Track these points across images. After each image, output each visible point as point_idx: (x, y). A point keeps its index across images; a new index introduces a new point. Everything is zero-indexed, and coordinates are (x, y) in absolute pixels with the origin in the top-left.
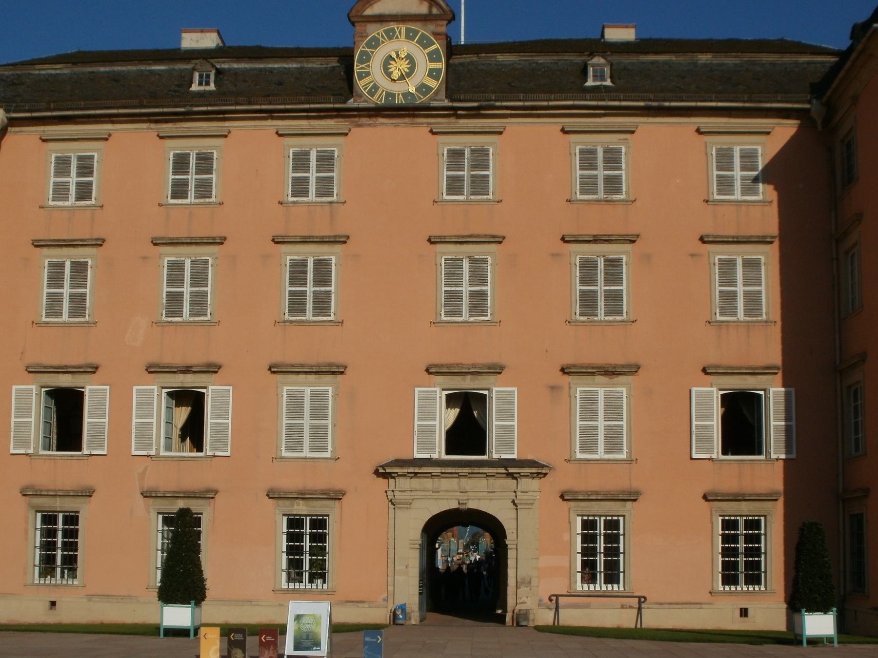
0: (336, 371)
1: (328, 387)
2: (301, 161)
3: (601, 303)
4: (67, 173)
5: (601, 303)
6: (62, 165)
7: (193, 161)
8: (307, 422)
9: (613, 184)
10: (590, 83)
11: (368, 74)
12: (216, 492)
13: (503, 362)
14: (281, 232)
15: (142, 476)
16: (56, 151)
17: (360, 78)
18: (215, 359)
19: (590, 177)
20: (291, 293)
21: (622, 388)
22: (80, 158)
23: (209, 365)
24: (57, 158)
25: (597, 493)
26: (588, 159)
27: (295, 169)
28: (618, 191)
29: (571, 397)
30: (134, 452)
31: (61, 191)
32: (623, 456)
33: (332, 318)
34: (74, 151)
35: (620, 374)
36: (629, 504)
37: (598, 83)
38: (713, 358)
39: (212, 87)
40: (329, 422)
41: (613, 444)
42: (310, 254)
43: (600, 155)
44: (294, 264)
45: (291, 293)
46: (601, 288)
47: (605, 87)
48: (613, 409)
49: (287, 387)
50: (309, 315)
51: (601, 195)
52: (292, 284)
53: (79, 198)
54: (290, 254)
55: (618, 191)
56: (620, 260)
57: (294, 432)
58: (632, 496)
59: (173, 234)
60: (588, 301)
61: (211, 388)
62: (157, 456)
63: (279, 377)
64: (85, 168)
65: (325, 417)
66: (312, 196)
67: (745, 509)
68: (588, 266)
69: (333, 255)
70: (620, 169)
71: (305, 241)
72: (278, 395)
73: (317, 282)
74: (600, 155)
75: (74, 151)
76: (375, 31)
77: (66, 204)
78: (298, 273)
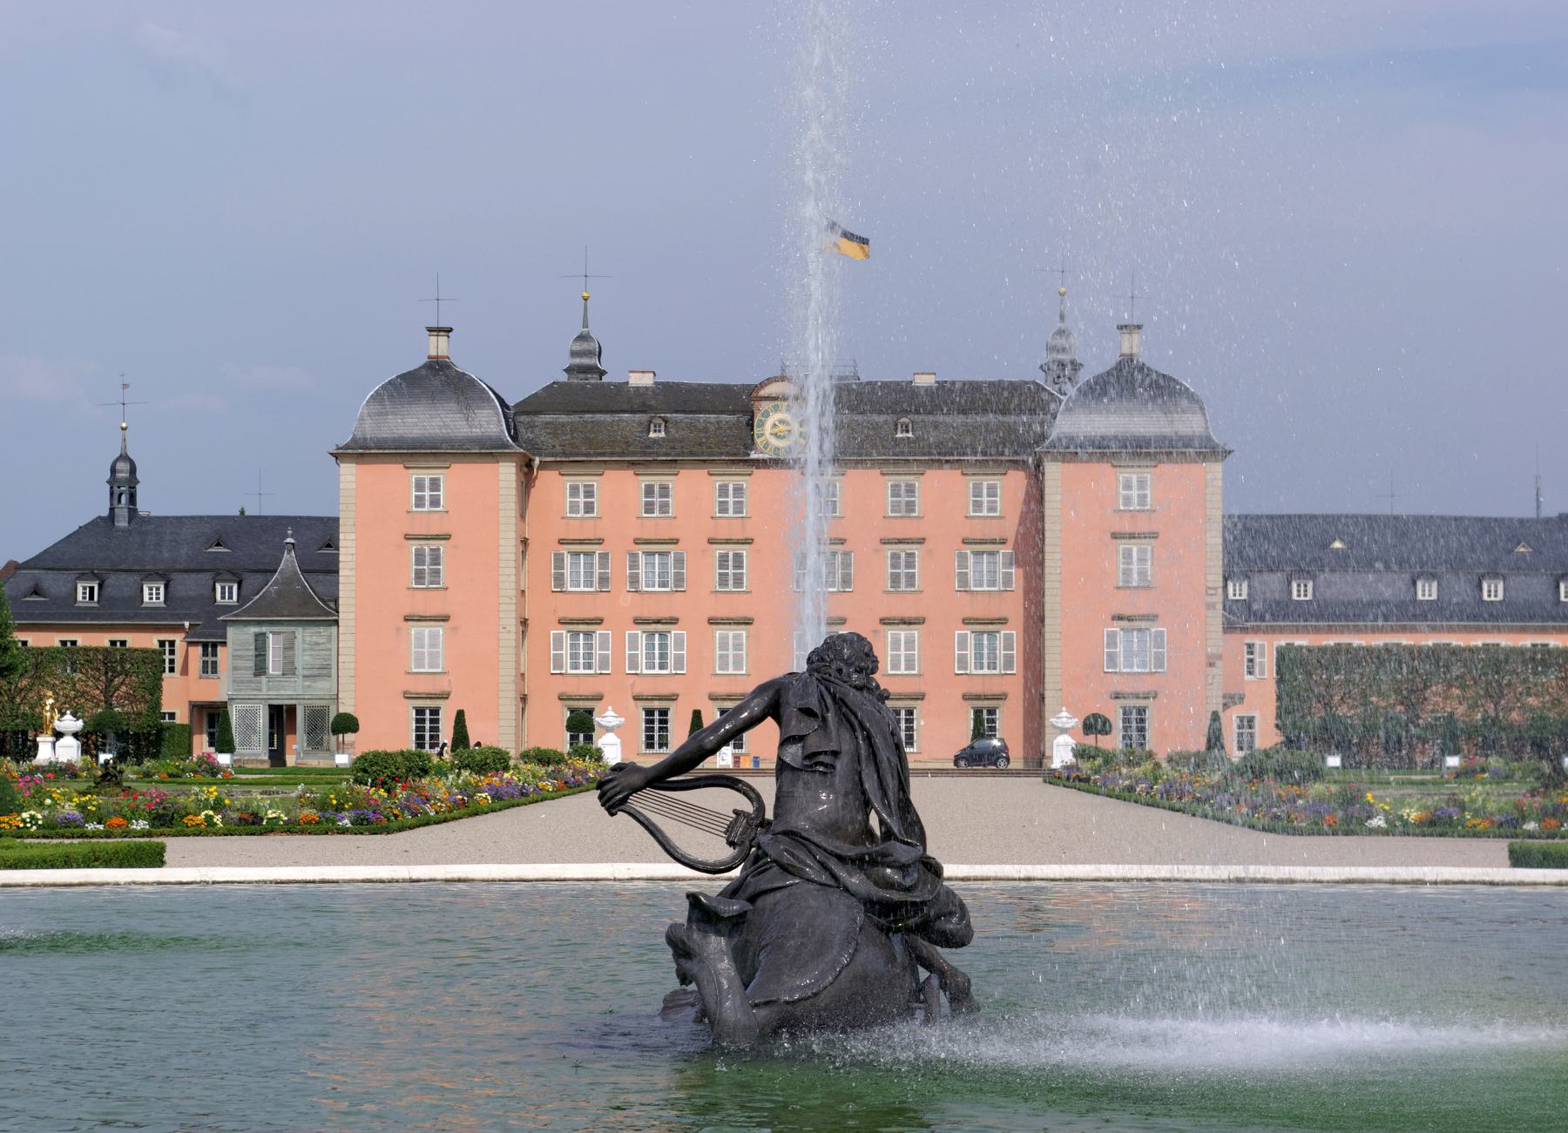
0: (747, 622)
1: (743, 632)
2: (723, 491)
3: (903, 580)
4: (578, 496)
5: (903, 580)
6: (574, 490)
7: (656, 489)
8: (731, 652)
9: (910, 506)
10: (899, 435)
11: (763, 435)
12: (678, 695)
13: (845, 615)
14: (712, 536)
15: (632, 686)
16: (570, 481)
17: (758, 437)
18: (674, 614)
19: (897, 502)
20: (720, 574)
21: (915, 632)
22: (585, 486)
23: (672, 619)
24: (571, 486)
25: (900, 694)
26: (896, 491)
27: (720, 496)
28: (913, 511)
29: (885, 637)
30: (628, 672)
31: (574, 508)
32: (915, 672)
33: (744, 589)
34: (581, 481)
35: (915, 623)
36: (919, 702)
37: (904, 435)
38: (969, 613)
39: (662, 435)
40: (744, 652)
41: (909, 666)
42: (731, 550)
43: (903, 488)
44: (721, 556)
45: (720, 574)
46: (903, 570)
47: (908, 438)
48: (910, 644)
49: (719, 632)
50: (731, 588)
51: (903, 514)
52: (720, 568)
53: (586, 512)
54: (719, 550)
55: (913, 511)
56: (914, 554)
57: (724, 658)
58: (920, 697)
59: (647, 536)
60: (895, 579)
61: (673, 632)
62: (642, 674)
63: (714, 627)
64: (589, 493)
65: (741, 650)
66: (731, 513)
67: (986, 704)
68: (895, 557)
69: (744, 551)
70: (914, 496)
71: (728, 542)
72: (713, 637)
73: (735, 567)
74: (903, 488)
75: (580, 481)
76: (765, 405)
77: (579, 516)
78: (723, 560)
